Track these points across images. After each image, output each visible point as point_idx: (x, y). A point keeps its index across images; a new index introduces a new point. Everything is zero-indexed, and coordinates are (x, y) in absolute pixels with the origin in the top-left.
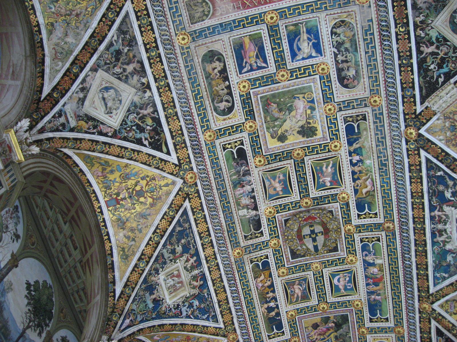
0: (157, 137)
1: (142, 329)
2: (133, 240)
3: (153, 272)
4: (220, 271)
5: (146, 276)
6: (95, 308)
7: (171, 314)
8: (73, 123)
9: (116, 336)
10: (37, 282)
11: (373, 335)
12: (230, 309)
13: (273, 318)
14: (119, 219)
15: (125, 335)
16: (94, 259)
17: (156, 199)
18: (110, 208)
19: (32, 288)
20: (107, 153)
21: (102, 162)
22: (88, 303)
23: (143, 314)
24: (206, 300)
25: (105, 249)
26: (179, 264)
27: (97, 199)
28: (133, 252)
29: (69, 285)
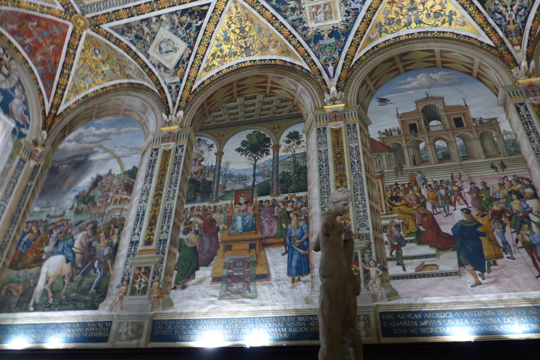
0: (196, 13)
2: (277, 42)
5: (305, 40)
6: (302, 95)
7: (351, 21)
8: (177, 79)
14: (261, 49)
16: (275, 81)
17: (248, 18)
18: (252, 54)
20: (203, 56)
21: (211, 58)
22: (293, 101)
23: (335, 50)
26: (306, 6)
27: (244, 62)
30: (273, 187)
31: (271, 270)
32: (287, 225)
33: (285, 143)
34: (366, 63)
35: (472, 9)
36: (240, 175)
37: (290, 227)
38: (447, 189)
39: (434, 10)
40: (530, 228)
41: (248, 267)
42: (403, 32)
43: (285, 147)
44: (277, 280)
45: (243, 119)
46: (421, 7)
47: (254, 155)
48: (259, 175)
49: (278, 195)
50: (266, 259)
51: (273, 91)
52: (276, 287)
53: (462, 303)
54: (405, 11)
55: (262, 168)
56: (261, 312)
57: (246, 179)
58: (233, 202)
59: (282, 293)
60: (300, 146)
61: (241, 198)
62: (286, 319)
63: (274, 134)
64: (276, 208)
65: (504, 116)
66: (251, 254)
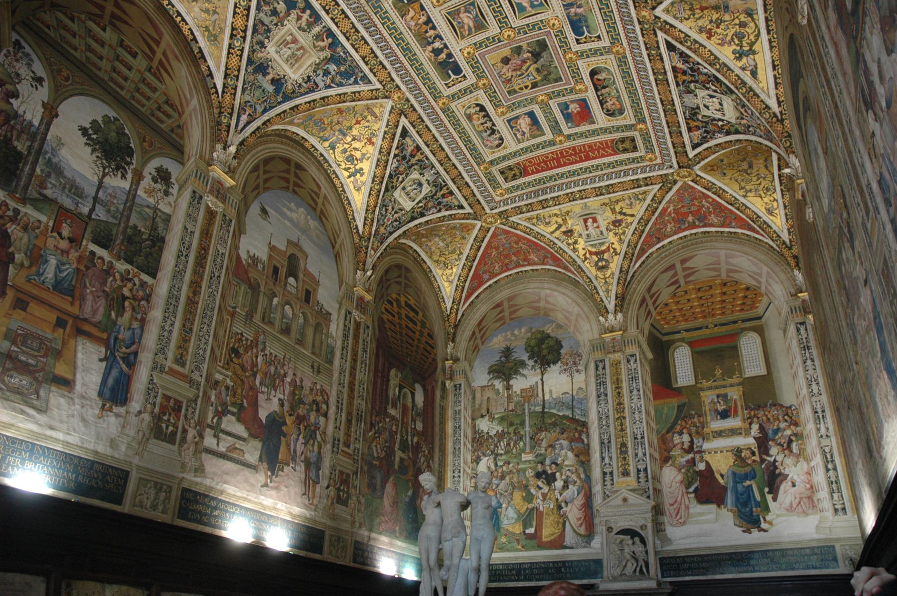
1: (268, 120)
2: (215, 12)
3: (257, 47)
4: (349, 19)
5: (249, 55)
6: (193, 116)
7: (302, 90)
9: (235, 139)
10: (94, 122)
11: (585, 60)
12: (381, 63)
13: (445, 61)
15: (247, 134)
16: (171, 56)
19: (90, 132)
22: (180, 115)
24: (345, 60)
25: (184, 35)
26: (289, 26)
28: (220, 28)
29: (143, 106)
30: (115, 240)
31: (78, 377)
32: (117, 317)
33: (150, 177)
34: (266, 142)
35: (377, 187)
36: (74, 181)
37: (120, 321)
38: (276, 368)
39: (353, 153)
40: (313, 445)
41: (45, 356)
42: (313, 141)
43: (150, 185)
44: (83, 397)
45: (106, 78)
46: (349, 139)
47: (104, 161)
48: (104, 205)
49: (119, 259)
50: (75, 356)
51: (162, 71)
52: (78, 407)
53: (249, 501)
54: (337, 127)
55: (110, 195)
56: (47, 438)
57: (81, 197)
58: (51, 224)
59: (84, 420)
60: (167, 200)
61: (64, 225)
62: (79, 462)
63: (142, 149)
64: (111, 279)
65: (336, 316)
66: (56, 335)
